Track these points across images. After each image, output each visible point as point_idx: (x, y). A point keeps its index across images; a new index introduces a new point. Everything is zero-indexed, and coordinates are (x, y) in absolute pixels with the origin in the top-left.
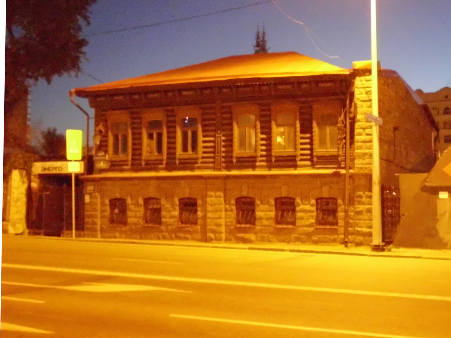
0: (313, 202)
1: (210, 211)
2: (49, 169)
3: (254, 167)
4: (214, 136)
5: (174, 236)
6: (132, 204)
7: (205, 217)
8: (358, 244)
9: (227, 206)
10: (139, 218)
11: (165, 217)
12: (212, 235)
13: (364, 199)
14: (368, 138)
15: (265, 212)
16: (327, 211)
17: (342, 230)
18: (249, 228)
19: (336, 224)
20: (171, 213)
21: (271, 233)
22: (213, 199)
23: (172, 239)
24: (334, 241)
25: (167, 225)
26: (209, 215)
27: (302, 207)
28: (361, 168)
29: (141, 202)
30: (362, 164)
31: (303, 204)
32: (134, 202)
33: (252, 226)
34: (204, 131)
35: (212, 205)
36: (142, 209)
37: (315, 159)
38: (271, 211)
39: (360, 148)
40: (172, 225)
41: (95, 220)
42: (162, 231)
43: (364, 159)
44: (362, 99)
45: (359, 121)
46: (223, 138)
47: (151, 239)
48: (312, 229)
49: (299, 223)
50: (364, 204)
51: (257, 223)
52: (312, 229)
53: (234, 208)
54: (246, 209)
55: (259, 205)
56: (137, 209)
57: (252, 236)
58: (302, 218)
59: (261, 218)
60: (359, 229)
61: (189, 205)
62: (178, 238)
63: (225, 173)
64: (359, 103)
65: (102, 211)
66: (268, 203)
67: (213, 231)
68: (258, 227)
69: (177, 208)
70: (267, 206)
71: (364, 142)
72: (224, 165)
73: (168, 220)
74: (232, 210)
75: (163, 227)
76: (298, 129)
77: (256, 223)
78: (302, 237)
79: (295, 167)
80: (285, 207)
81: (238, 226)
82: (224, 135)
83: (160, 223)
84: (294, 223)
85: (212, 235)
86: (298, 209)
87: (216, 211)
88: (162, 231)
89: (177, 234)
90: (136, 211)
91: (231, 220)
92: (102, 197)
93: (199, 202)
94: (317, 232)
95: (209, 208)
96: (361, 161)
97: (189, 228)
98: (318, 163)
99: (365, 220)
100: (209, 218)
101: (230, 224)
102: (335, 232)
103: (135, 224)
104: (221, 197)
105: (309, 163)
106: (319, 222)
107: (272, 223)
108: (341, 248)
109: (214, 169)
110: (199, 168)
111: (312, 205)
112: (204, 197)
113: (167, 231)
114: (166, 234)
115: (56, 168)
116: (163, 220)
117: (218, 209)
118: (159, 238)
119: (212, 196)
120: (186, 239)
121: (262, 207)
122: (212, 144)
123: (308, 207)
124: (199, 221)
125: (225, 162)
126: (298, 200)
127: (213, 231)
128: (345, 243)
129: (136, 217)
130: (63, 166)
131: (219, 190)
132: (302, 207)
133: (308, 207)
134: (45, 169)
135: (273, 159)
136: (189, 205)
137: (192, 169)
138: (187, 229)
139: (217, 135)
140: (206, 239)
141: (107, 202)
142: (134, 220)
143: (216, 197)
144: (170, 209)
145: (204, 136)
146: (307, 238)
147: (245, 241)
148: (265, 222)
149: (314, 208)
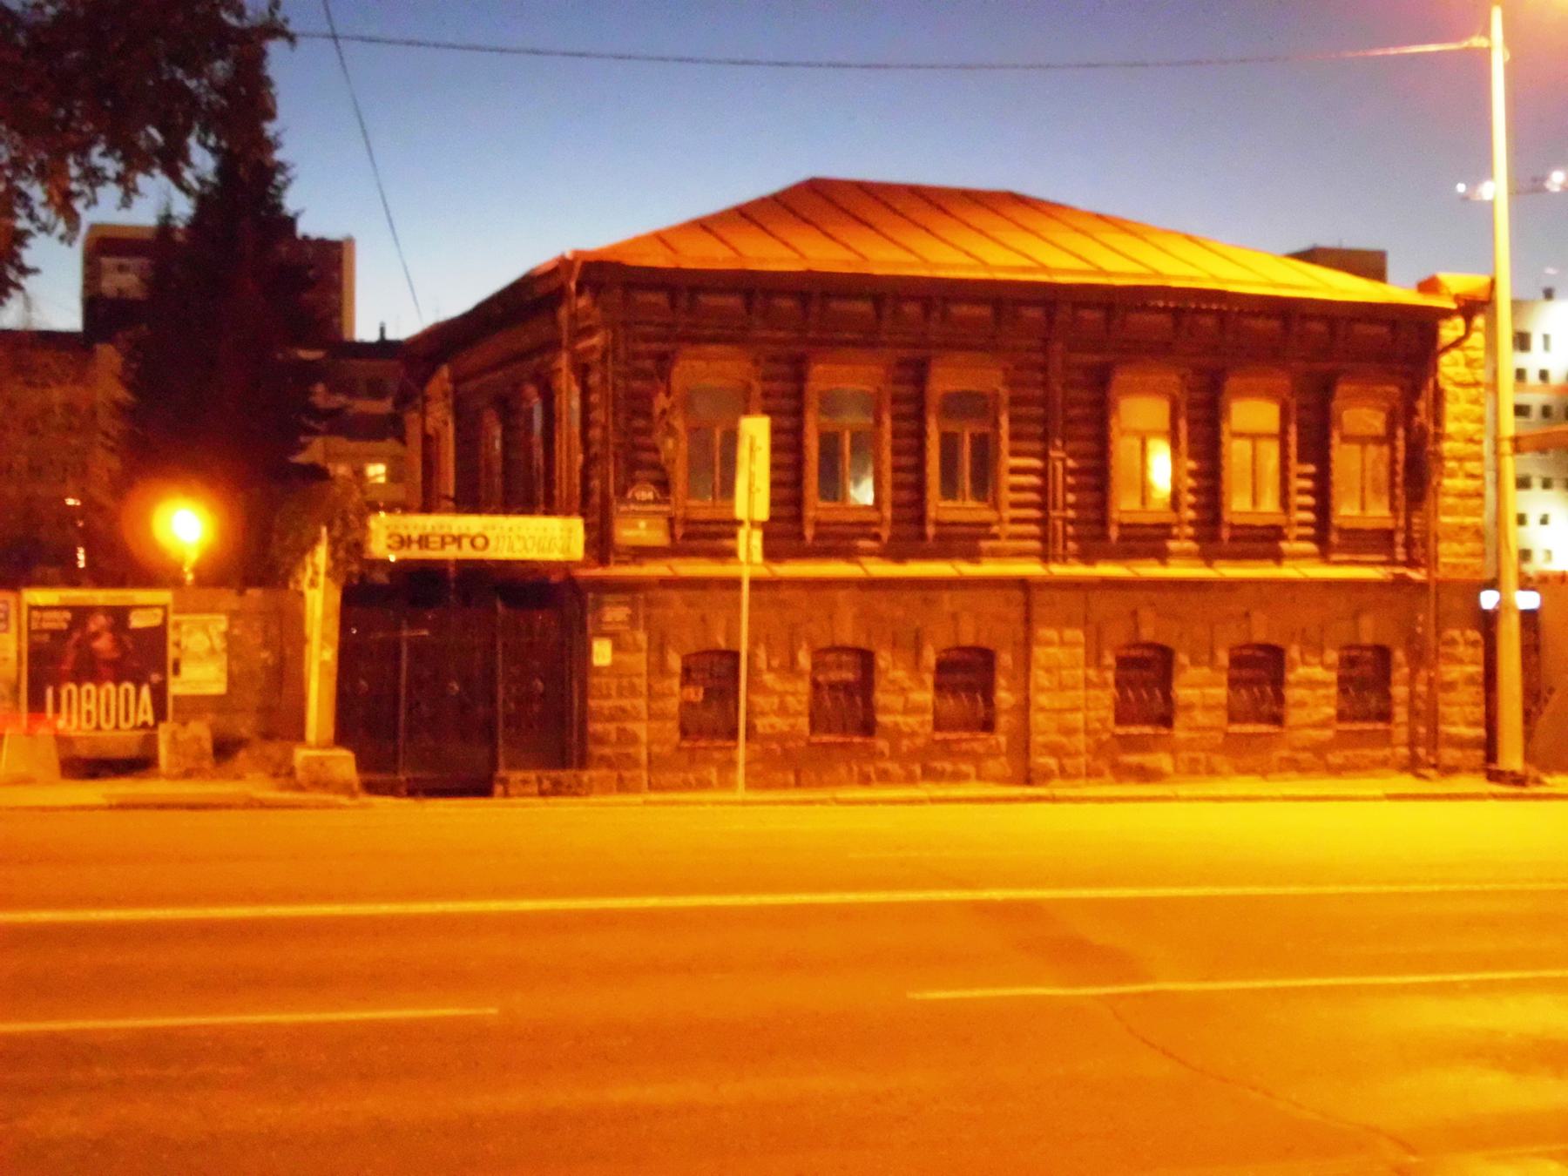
0: (1332, 656)
1: (1042, 690)
2: (423, 541)
3: (1162, 556)
4: (1044, 456)
5: (918, 769)
6: (770, 668)
7: (1024, 707)
8: (1449, 771)
9: (1092, 673)
10: (798, 714)
11: (887, 710)
12: (1051, 762)
13: (1461, 650)
14: (1471, 484)
15: (1200, 688)
16: (1366, 681)
17: (1401, 733)
18: (1156, 736)
19: (1386, 716)
20: (907, 698)
21: (1215, 750)
22: (1051, 650)
23: (910, 779)
24: (1384, 763)
25: (896, 734)
26: (1042, 699)
27: (1302, 671)
28: (1455, 567)
29: (804, 660)
30: (1457, 555)
31: (1305, 663)
32: (775, 663)
33: (1163, 731)
34: (1014, 437)
35: (1048, 670)
36: (804, 686)
37: (1334, 538)
38: (1218, 685)
39: (1451, 511)
40: (913, 734)
41: (631, 726)
42: (875, 755)
43: (1461, 542)
44: (1458, 379)
45: (1450, 437)
46: (1071, 463)
47: (839, 783)
48: (1328, 734)
49: (1294, 716)
50: (1460, 661)
51: (1180, 721)
52: (1328, 734)
53: (1110, 676)
54: (1145, 681)
55: (1183, 667)
56: (789, 687)
57: (1163, 761)
58: (1302, 704)
59: (1189, 707)
60: (1453, 730)
61: (968, 674)
62: (930, 775)
63: (1078, 570)
64: (1449, 388)
65: (652, 695)
66: (1212, 662)
67: (1055, 750)
68: (1180, 733)
69: (929, 679)
70: (1206, 671)
71: (1463, 495)
72: (1072, 545)
73: (900, 719)
74: (1103, 685)
75: (882, 744)
76: (1293, 450)
77: (1177, 724)
78: (1302, 756)
79: (1278, 557)
80: (1260, 674)
81: (1120, 731)
82: (1072, 455)
83: (868, 727)
84: (1277, 720)
85: (1051, 762)
86: (1291, 677)
87: (1062, 687)
88: (875, 755)
89: (927, 764)
90: (782, 695)
91: (1103, 713)
92: (659, 647)
93: (1005, 659)
94: (1342, 740)
95: (1040, 677)
96: (1456, 547)
97: (979, 742)
98: (1341, 549)
99: (1460, 705)
100: (1042, 709)
101: (1098, 725)
102: (1386, 739)
103: (781, 738)
104: (1073, 644)
105: (1309, 547)
106: (1341, 716)
107: (1219, 718)
108: (1407, 783)
109: (1045, 557)
110: (996, 554)
111: (1328, 667)
112: (1026, 645)
113: (895, 755)
114: (893, 767)
115: (457, 540)
116: (883, 719)
117: (1064, 681)
118: (865, 781)
119: (1049, 643)
120: (958, 777)
121: (1194, 673)
122: (1033, 480)
123: (1318, 673)
124: (1003, 721)
125: (1077, 538)
126: (1294, 652)
127: (1055, 750)
128: (1412, 766)
129: (783, 710)
130: (489, 534)
131: (1069, 622)
132: (1302, 671)
133: (1318, 673)
134: (405, 542)
135: (1225, 533)
136: (968, 674)
137: (973, 556)
138: (964, 746)
139: (1053, 454)
140: (1028, 777)
141: (675, 662)
142: (781, 724)
143: (1063, 643)
144: (907, 684)
145: (1015, 453)
146: (1317, 760)
147: (1146, 775)
148: (1200, 718)
149: (1332, 676)
